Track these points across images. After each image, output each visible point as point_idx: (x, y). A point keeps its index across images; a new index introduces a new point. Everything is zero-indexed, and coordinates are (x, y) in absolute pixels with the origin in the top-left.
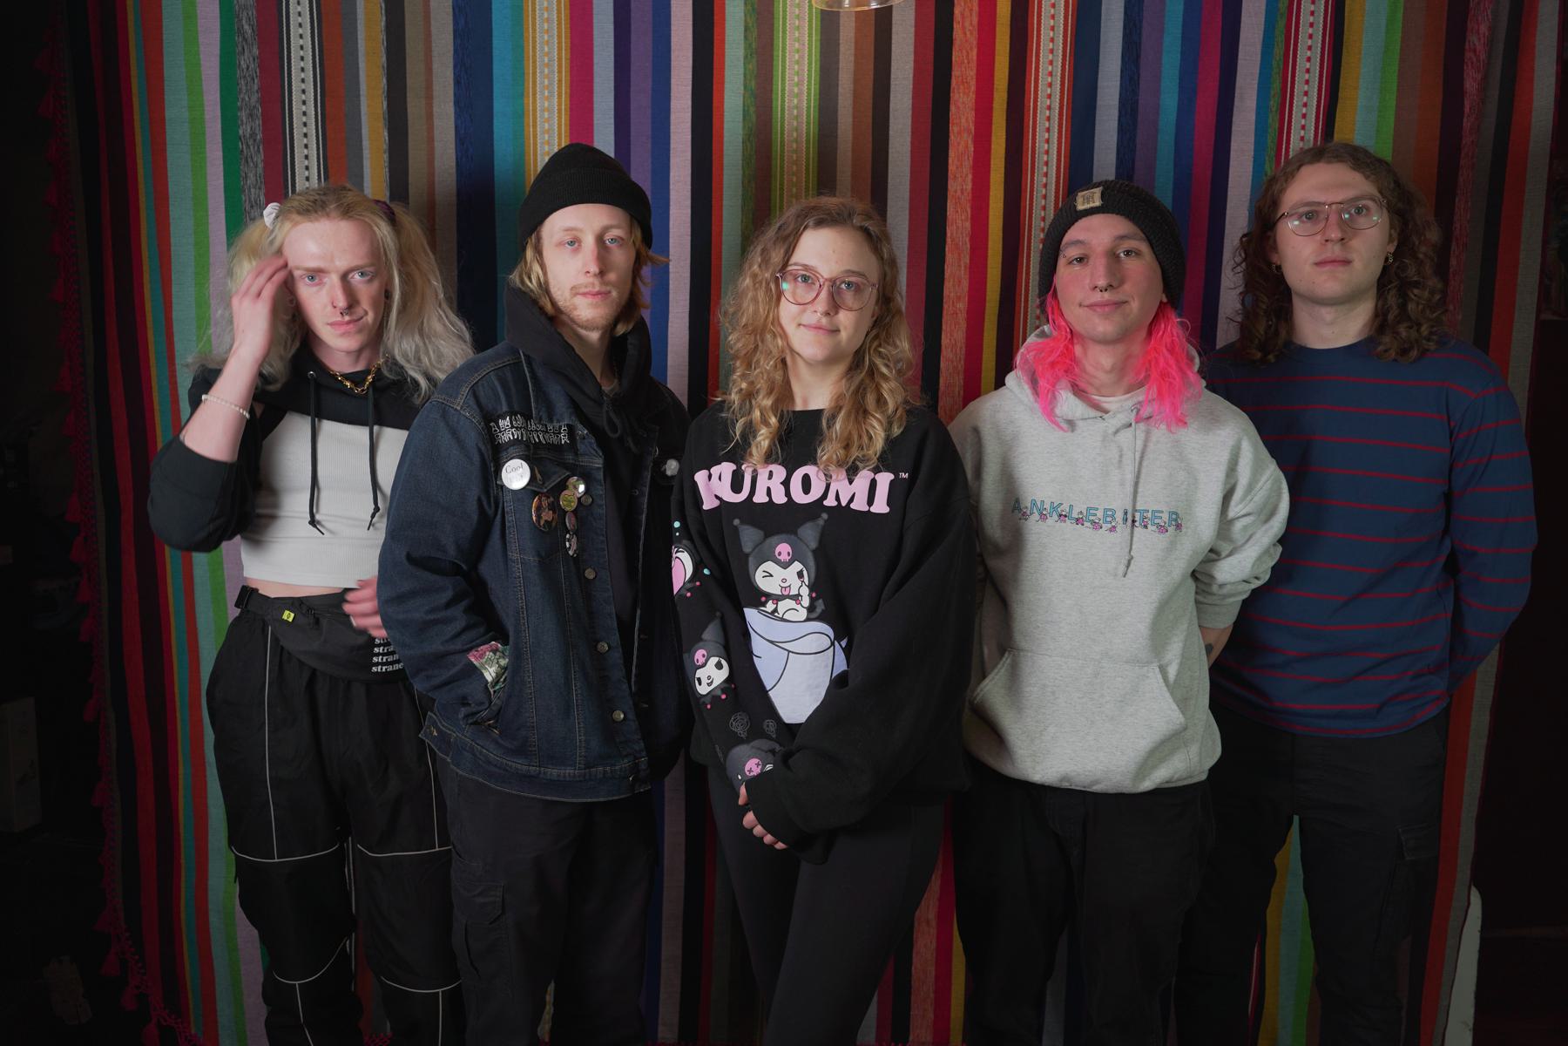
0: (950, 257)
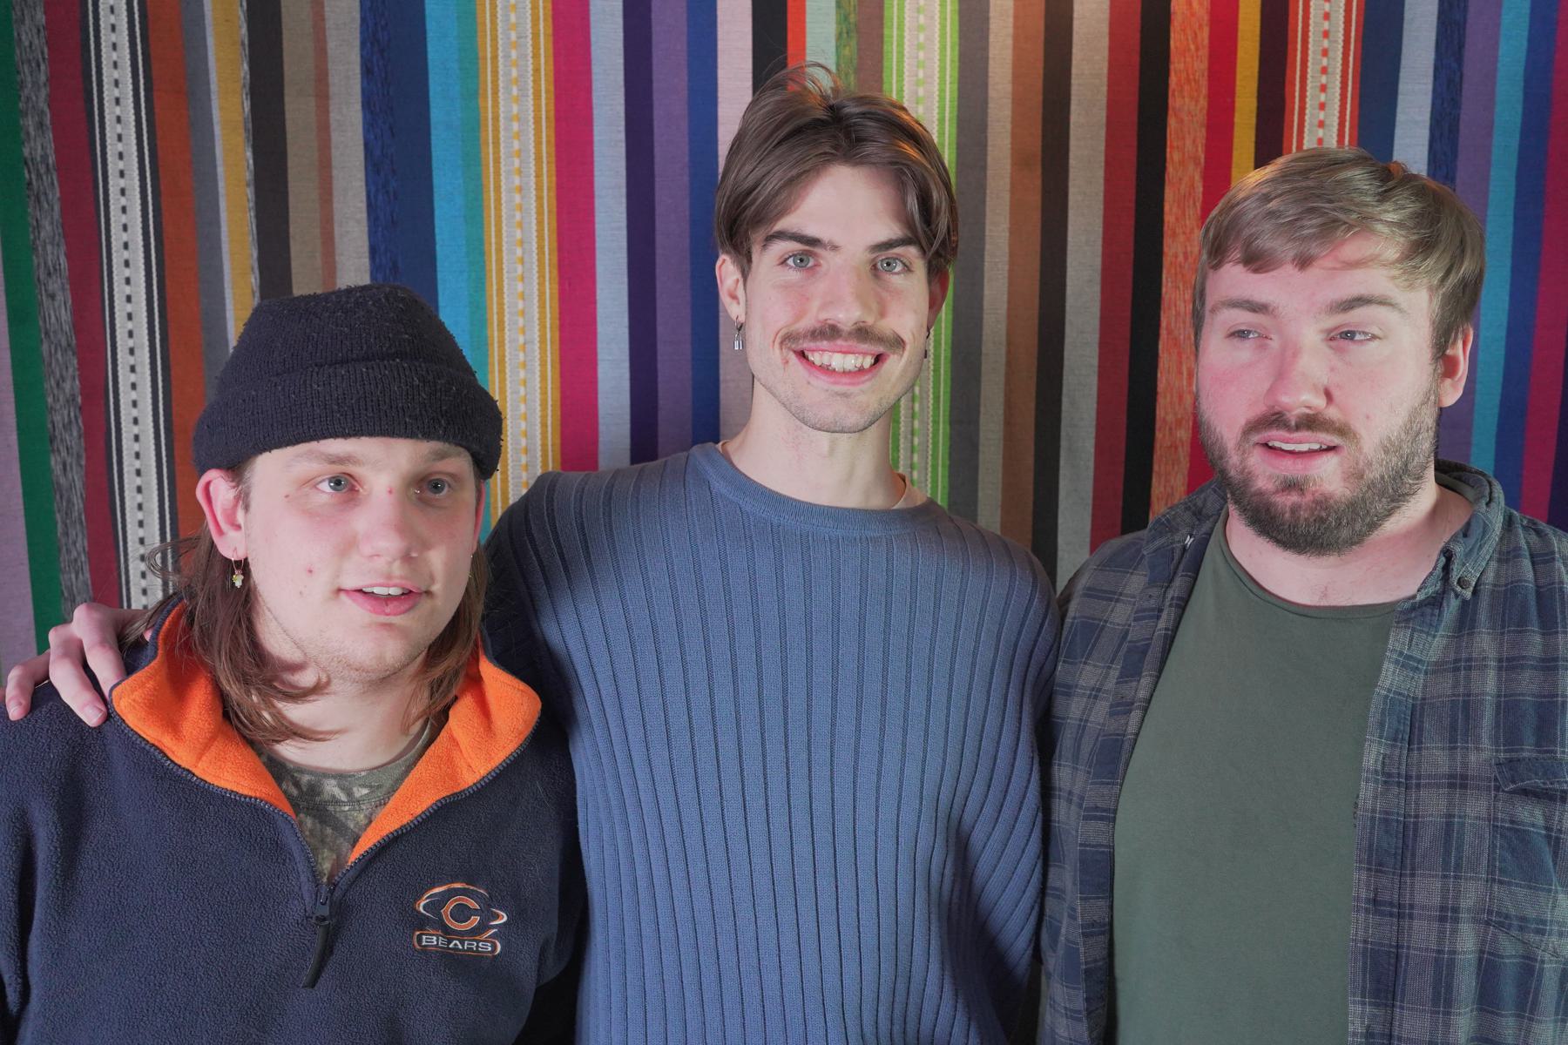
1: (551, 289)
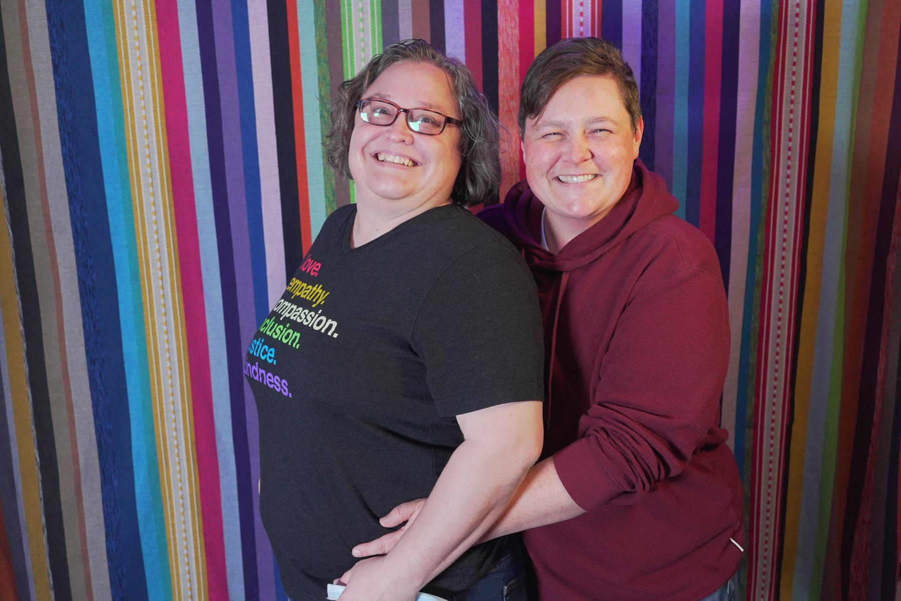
1: (154, 34)
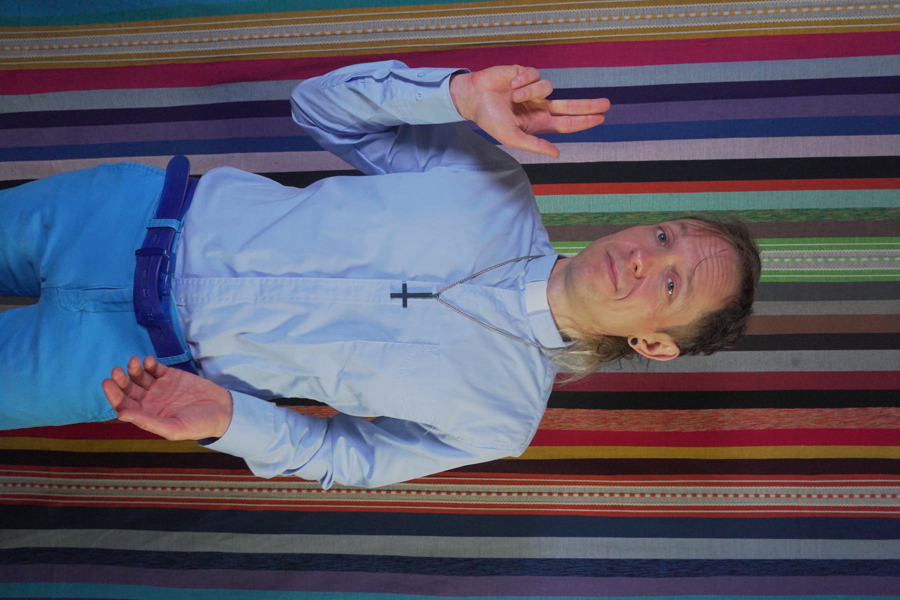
0: (659, 414)
1: (702, 34)
